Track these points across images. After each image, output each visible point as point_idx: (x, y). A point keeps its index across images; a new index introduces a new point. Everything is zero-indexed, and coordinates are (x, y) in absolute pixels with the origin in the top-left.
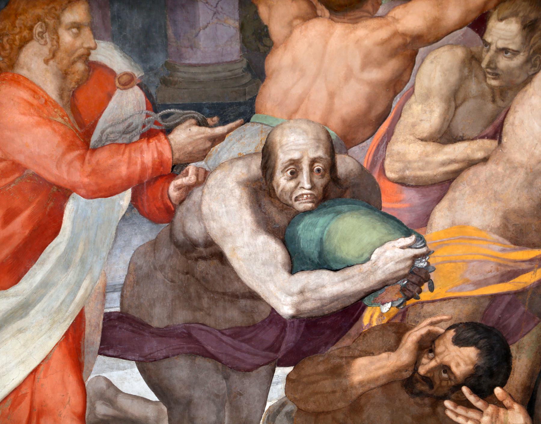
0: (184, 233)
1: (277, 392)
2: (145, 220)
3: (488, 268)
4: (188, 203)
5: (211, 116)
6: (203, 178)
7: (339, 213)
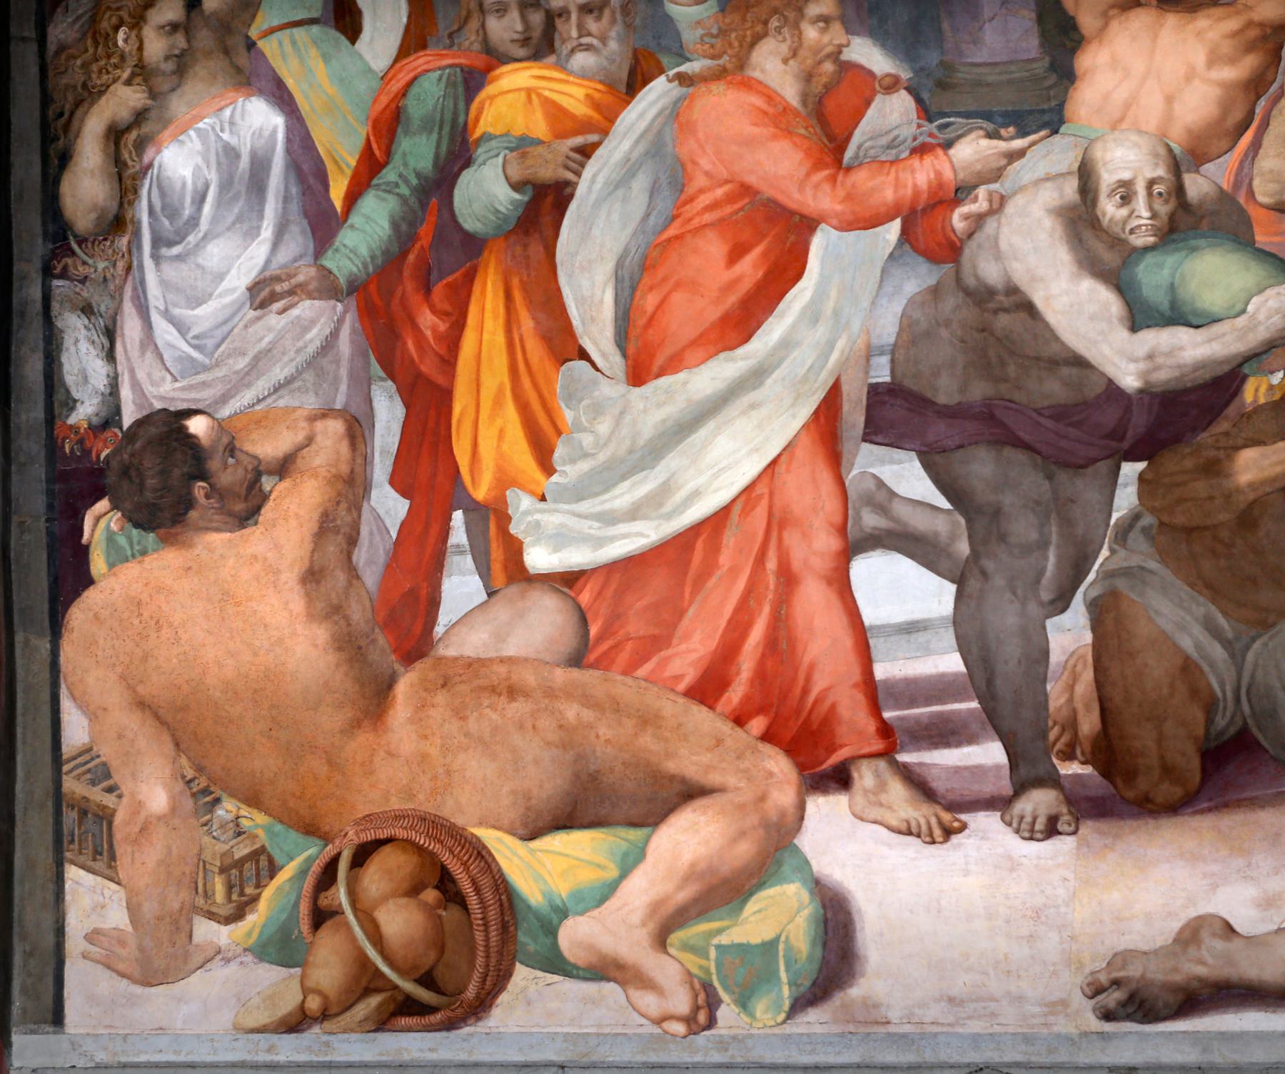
0: (977, 277)
2: (921, 259)
4: (979, 237)
5: (1006, 126)
6: (998, 205)
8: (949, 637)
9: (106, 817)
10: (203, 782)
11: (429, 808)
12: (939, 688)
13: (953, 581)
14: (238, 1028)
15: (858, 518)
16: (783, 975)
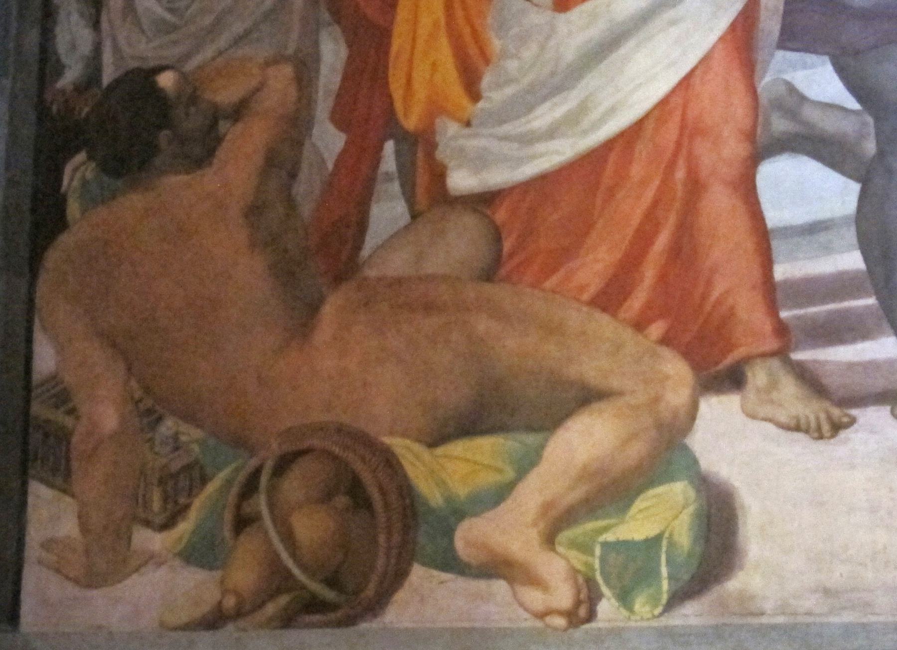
8: (851, 235)
9: (64, 437)
10: (149, 403)
11: (345, 419)
13: (857, 180)
14: (162, 624)
15: (767, 123)
16: (664, 571)
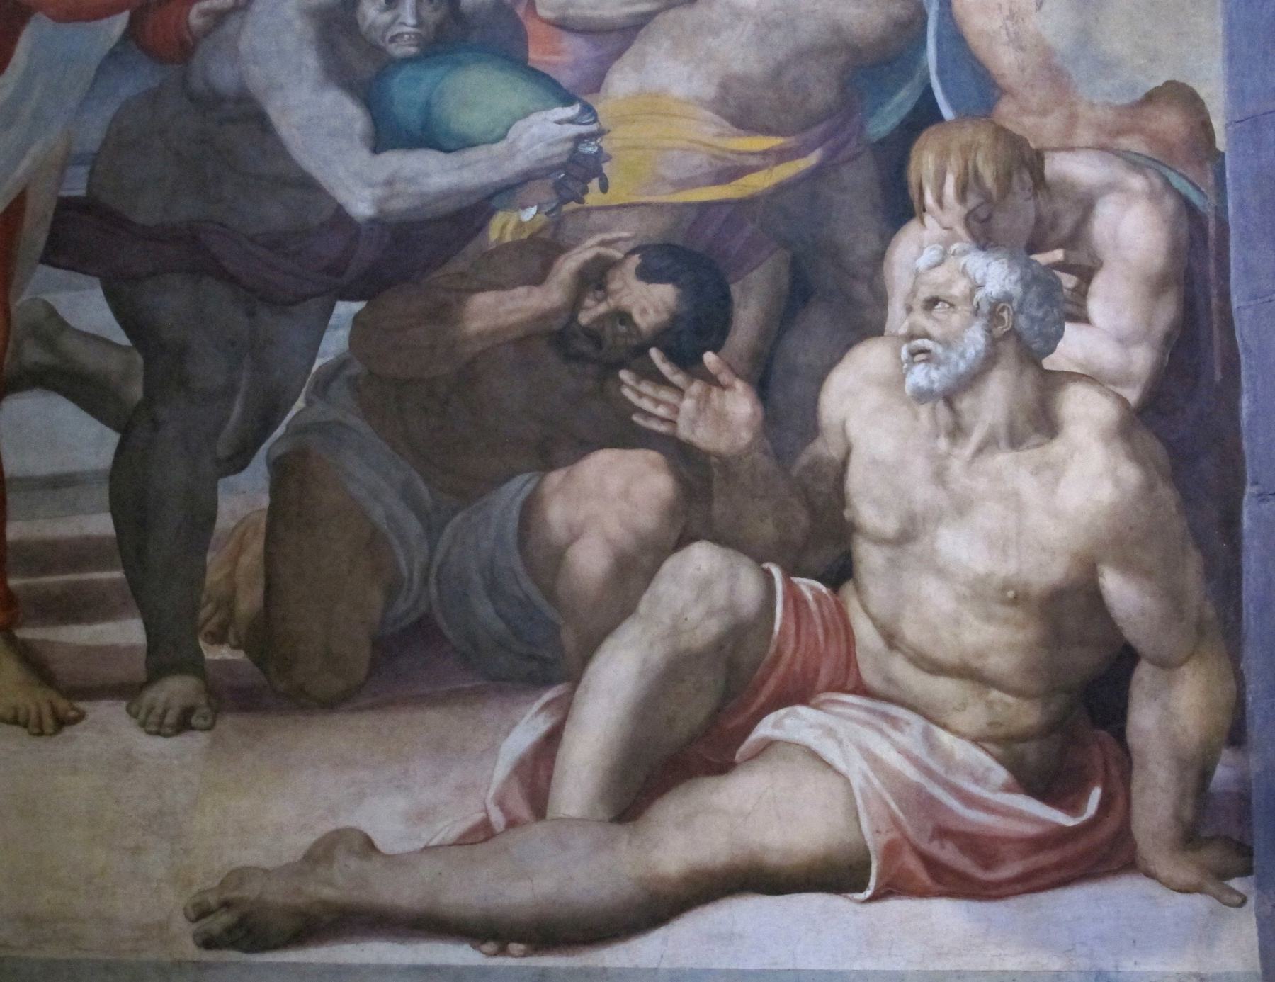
0: (207, 83)
1: (335, 343)
3: (696, 160)
7: (458, 64)
8: (102, 494)
12: (80, 554)
